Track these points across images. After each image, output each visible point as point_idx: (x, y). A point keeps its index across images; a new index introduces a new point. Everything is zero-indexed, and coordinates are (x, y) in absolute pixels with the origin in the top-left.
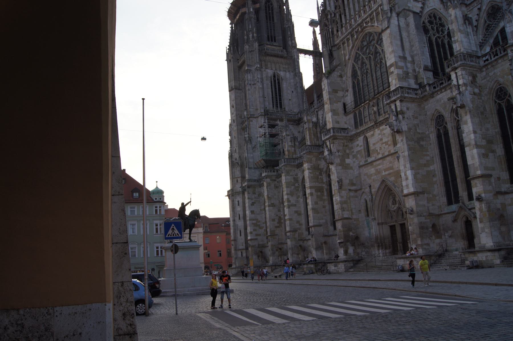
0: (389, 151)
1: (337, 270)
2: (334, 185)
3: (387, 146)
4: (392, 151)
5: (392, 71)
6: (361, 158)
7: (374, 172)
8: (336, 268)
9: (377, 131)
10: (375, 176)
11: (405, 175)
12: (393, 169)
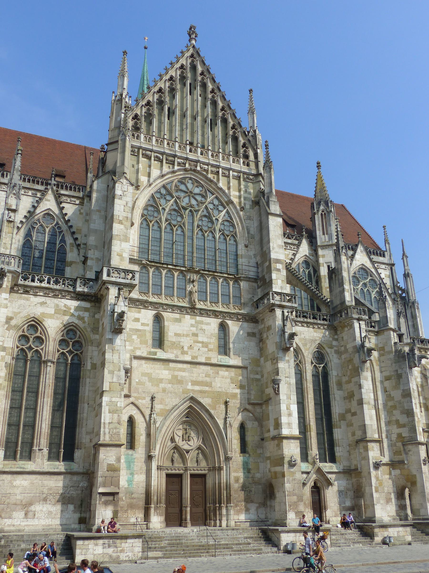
0: (210, 358)
1: (114, 555)
2: (112, 372)
3: (206, 349)
4: (214, 361)
5: (278, 268)
6: (140, 344)
7: (170, 377)
8: (110, 551)
9: (188, 319)
10: (170, 385)
11: (287, 409)
12: (211, 386)
